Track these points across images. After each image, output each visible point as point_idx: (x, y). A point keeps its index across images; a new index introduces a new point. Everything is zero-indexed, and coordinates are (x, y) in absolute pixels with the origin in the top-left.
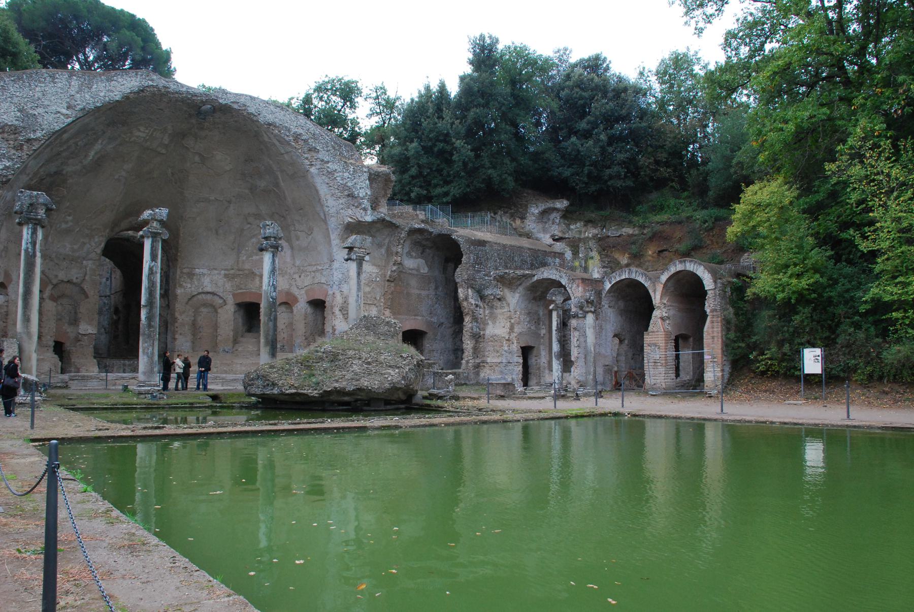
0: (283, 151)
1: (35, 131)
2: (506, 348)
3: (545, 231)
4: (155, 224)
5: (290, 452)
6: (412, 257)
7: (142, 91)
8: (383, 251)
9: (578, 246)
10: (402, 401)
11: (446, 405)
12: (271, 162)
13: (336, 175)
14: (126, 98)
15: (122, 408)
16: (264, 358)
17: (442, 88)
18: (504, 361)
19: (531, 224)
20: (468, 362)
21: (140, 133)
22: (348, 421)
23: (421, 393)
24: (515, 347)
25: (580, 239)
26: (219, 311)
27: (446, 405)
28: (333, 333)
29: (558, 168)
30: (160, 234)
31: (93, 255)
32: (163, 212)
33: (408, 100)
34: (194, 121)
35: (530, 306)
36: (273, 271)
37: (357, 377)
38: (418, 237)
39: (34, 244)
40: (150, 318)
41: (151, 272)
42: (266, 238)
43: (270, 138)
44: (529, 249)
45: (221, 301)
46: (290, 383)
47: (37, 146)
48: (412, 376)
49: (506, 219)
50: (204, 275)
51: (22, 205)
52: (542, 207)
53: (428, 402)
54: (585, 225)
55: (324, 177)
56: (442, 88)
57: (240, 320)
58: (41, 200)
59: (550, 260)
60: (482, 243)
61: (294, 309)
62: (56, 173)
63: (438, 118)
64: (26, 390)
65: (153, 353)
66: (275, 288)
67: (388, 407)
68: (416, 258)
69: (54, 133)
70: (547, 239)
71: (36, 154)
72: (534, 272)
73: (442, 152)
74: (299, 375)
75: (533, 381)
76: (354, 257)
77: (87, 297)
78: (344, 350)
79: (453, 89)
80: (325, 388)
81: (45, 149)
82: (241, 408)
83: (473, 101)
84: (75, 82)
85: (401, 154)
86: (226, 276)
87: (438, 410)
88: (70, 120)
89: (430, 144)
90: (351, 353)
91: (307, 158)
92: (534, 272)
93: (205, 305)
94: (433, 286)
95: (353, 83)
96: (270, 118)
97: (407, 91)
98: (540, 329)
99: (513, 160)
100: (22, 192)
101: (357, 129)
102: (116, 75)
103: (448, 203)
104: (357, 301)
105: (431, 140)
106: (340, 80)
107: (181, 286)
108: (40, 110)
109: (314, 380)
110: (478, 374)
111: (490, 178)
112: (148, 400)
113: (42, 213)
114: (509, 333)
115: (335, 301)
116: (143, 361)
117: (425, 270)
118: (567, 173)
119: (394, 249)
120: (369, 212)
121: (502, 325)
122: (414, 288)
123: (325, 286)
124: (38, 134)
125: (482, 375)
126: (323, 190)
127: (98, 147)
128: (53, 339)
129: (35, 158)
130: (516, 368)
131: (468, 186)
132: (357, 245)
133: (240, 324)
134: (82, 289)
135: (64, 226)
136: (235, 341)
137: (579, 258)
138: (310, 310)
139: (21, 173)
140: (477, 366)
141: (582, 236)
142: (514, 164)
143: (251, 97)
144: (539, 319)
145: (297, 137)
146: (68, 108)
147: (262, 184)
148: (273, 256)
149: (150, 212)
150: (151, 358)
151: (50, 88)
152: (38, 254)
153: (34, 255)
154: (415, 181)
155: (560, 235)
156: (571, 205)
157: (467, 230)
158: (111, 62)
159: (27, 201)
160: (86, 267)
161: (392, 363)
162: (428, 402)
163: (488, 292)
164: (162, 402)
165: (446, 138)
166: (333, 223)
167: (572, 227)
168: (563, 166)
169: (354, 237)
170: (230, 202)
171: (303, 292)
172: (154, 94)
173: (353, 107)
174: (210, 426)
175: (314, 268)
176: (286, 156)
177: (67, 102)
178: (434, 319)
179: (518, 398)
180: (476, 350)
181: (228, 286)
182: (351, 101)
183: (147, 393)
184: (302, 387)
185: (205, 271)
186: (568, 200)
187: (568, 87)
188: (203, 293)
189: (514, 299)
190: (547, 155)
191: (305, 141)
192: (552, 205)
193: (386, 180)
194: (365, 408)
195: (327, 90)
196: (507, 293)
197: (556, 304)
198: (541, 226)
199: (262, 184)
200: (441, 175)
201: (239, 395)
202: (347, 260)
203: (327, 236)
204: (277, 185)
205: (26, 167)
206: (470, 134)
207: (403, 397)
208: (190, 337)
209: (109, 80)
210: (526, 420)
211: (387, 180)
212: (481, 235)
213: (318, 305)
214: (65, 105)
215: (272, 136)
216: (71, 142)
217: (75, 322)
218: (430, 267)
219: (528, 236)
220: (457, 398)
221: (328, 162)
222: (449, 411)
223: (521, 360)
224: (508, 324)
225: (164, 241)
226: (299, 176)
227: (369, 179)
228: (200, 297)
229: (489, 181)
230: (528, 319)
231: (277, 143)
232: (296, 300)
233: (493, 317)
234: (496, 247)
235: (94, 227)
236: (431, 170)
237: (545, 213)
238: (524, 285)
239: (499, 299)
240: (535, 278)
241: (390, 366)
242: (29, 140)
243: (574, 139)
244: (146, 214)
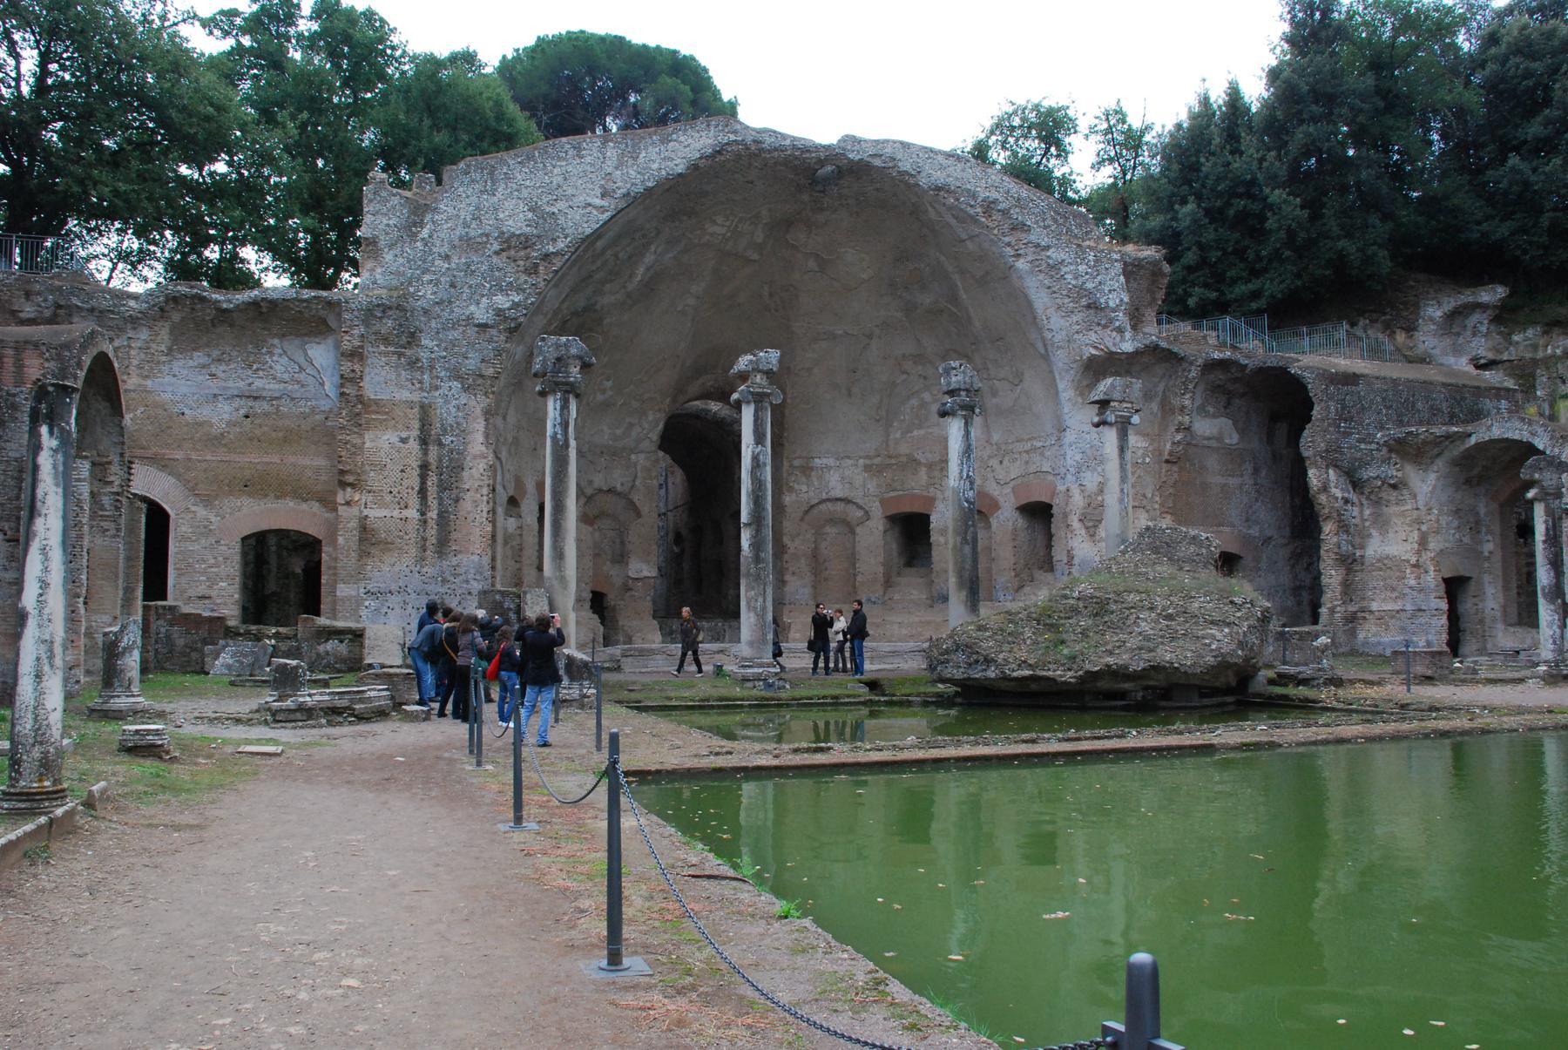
0: (964, 236)
1: (554, 240)
2: (1412, 582)
3: (1457, 351)
4: (758, 379)
5: (1007, 788)
6: (1207, 415)
7: (719, 152)
8: (1155, 406)
9: (1533, 376)
10: (1230, 691)
11: (1325, 695)
12: (943, 258)
13: (1065, 269)
14: (694, 167)
15: (719, 707)
16: (956, 613)
17: (1234, 95)
18: (1409, 607)
19: (1427, 339)
20: (1332, 611)
21: (717, 228)
22: (1170, 732)
23: (1264, 674)
24: (1432, 579)
25: (1535, 362)
26: (858, 530)
27: (1325, 695)
28: (1070, 563)
29: (1479, 223)
30: (768, 395)
31: (646, 444)
32: (771, 357)
33: (1170, 127)
34: (805, 197)
35: (1458, 496)
36: (967, 451)
37: (1148, 645)
38: (1219, 376)
39: (565, 425)
40: (757, 546)
41: (757, 463)
42: (951, 393)
43: (939, 214)
44: (1444, 385)
45: (860, 513)
46: (1018, 658)
47: (559, 264)
48: (1254, 639)
49: (1376, 334)
50: (829, 468)
51: (544, 360)
52: (1450, 303)
53: (1279, 690)
54: (1545, 333)
55: (1041, 277)
56: (1234, 95)
57: (894, 546)
58: (573, 351)
59: (1488, 404)
60: (1351, 379)
61: (994, 523)
62: (585, 309)
63: (1232, 153)
64: (572, 679)
65: (764, 608)
66: (972, 483)
67: (1206, 701)
68: (1214, 416)
69: (583, 240)
70: (1463, 364)
71: (558, 278)
72: (1469, 428)
73: (1244, 216)
74: (1035, 643)
75: (1469, 646)
76: (1111, 418)
77: (639, 515)
78: (1118, 594)
79: (1255, 92)
80: (1088, 667)
81: (570, 268)
82: (926, 704)
83: (1300, 112)
84: (612, 152)
85: (1164, 228)
86: (867, 468)
87: (1307, 707)
88: (607, 215)
89: (1219, 203)
90: (1132, 598)
91: (1009, 244)
92: (1469, 428)
93: (832, 521)
94: (1249, 467)
95: (1059, 110)
96: (939, 177)
97: (1164, 111)
98: (1480, 542)
99: (1386, 217)
100: (543, 339)
101: (1070, 194)
102: (675, 131)
103: (1259, 312)
104: (1121, 501)
105: (1220, 195)
106: (1036, 107)
107: (791, 489)
108: (561, 205)
109: (1066, 651)
110: (1352, 633)
111: (1342, 256)
112: (759, 691)
113: (575, 371)
114: (1419, 552)
115: (1072, 500)
116: (747, 620)
117: (1233, 438)
118: (1503, 230)
119: (1176, 402)
120: (1128, 335)
121: (1402, 539)
122: (1215, 473)
123: (1050, 478)
124: (561, 245)
125: (1361, 636)
126: (1041, 300)
127: (649, 258)
128: (589, 589)
129: (556, 286)
130: (1434, 621)
131: (1298, 276)
132: (1117, 395)
133: (895, 553)
134: (631, 503)
135: (600, 397)
136: (888, 583)
137: (1536, 398)
138: (1021, 522)
139: (535, 313)
140: (1352, 619)
141: (1540, 355)
142: (1390, 225)
143: (902, 143)
144: (1477, 523)
145: (989, 206)
146: (603, 196)
147: (926, 299)
148: (966, 424)
149: (750, 357)
150: (761, 616)
151: (574, 167)
152: (573, 443)
153: (566, 445)
154: (1192, 277)
155: (1491, 356)
156: (1511, 295)
157: (1314, 357)
158: (660, 118)
159: (552, 355)
160: (635, 465)
161: (1216, 616)
162: (1279, 690)
163: (1369, 473)
164: (783, 695)
165: (1248, 188)
166: (1061, 359)
167: (1516, 338)
168: (1488, 218)
169: (1109, 381)
170: (870, 337)
171: (1008, 490)
172: (738, 156)
173: (1063, 153)
174: (913, 747)
175: (1028, 446)
176: (969, 244)
177: (602, 186)
178: (1254, 531)
179: (1464, 681)
180: (1348, 588)
181: (872, 486)
182: (1059, 144)
183: (757, 678)
184: (1043, 667)
185: (831, 462)
186: (1502, 283)
187: (1495, 59)
188: (828, 500)
189: (1426, 484)
190: (1456, 201)
191: (1005, 212)
192: (1471, 299)
193: (1154, 274)
194: (1163, 703)
195: (1013, 129)
196: (1412, 473)
197: (1542, 488)
198: (1447, 341)
199: (926, 299)
200: (1243, 260)
201: (914, 682)
202: (1097, 425)
203: (1052, 384)
204: (954, 299)
205: (542, 302)
206: (1296, 178)
207: (1233, 682)
208: (809, 578)
209: (665, 140)
210: (1531, 729)
211: (1156, 273)
212: (1343, 362)
213: (1039, 513)
214: (598, 192)
215: (942, 210)
216: (609, 252)
217: (621, 558)
218: (1242, 432)
219: (1423, 360)
220: (1338, 682)
221: (1048, 248)
222: (1333, 710)
223: (1444, 606)
224: (1416, 534)
225: (775, 408)
226: (994, 276)
227: (1125, 273)
228: (823, 507)
229: (1340, 263)
230: (1456, 523)
231: (953, 222)
232: (995, 506)
233: (1383, 524)
234: (1378, 385)
235: (647, 396)
236: (1225, 253)
237: (1455, 315)
238: (1447, 455)
239: (1394, 487)
240: (1473, 440)
241: (1212, 623)
242: (546, 257)
243: (1513, 160)
244: (744, 362)
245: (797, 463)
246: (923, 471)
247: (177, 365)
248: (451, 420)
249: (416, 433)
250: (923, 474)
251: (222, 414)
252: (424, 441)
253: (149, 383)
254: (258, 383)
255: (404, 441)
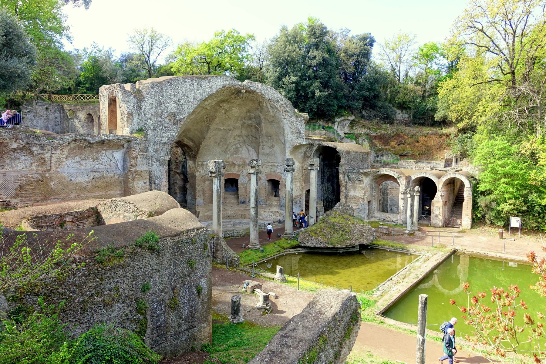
0: (271, 111)
24: (366, 202)
107: (198, 171)
126: (287, 130)
170: (230, 130)
189: (367, 180)
204: (259, 124)
226: (276, 122)
231: (269, 107)
242: (180, 120)
245: (199, 163)
246: (237, 167)
247: (70, 162)
248: (157, 175)
249: (148, 180)
250: (237, 167)
251: (84, 179)
252: (150, 183)
253: (59, 170)
254: (96, 166)
255: (145, 183)
